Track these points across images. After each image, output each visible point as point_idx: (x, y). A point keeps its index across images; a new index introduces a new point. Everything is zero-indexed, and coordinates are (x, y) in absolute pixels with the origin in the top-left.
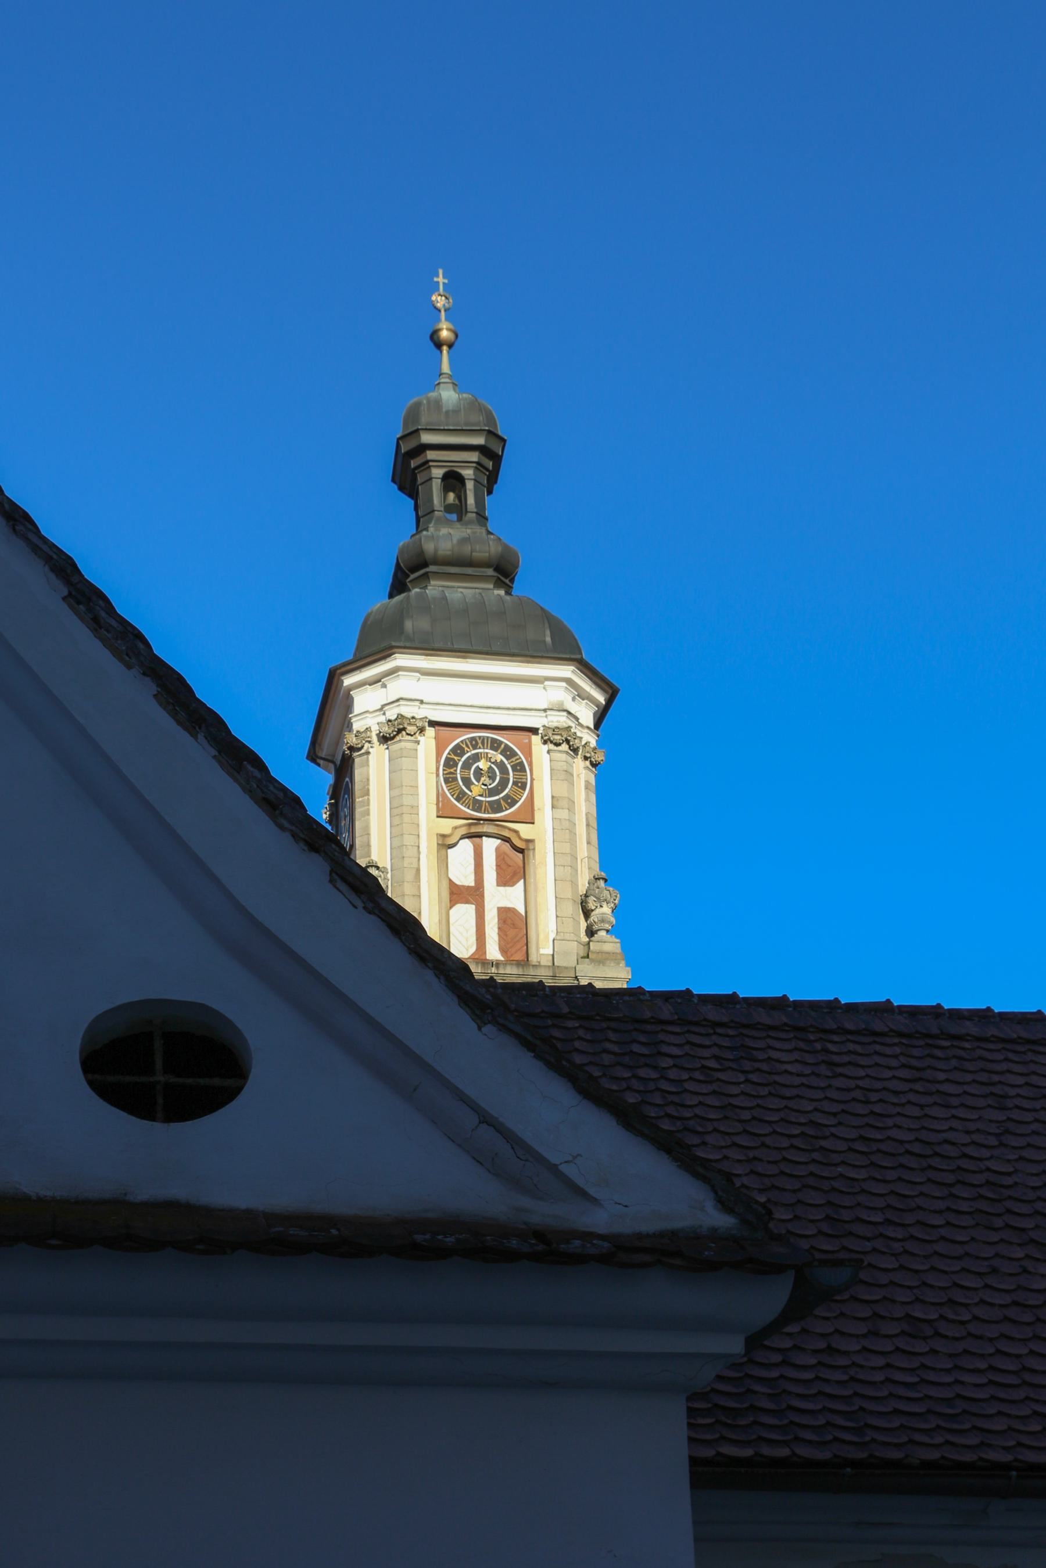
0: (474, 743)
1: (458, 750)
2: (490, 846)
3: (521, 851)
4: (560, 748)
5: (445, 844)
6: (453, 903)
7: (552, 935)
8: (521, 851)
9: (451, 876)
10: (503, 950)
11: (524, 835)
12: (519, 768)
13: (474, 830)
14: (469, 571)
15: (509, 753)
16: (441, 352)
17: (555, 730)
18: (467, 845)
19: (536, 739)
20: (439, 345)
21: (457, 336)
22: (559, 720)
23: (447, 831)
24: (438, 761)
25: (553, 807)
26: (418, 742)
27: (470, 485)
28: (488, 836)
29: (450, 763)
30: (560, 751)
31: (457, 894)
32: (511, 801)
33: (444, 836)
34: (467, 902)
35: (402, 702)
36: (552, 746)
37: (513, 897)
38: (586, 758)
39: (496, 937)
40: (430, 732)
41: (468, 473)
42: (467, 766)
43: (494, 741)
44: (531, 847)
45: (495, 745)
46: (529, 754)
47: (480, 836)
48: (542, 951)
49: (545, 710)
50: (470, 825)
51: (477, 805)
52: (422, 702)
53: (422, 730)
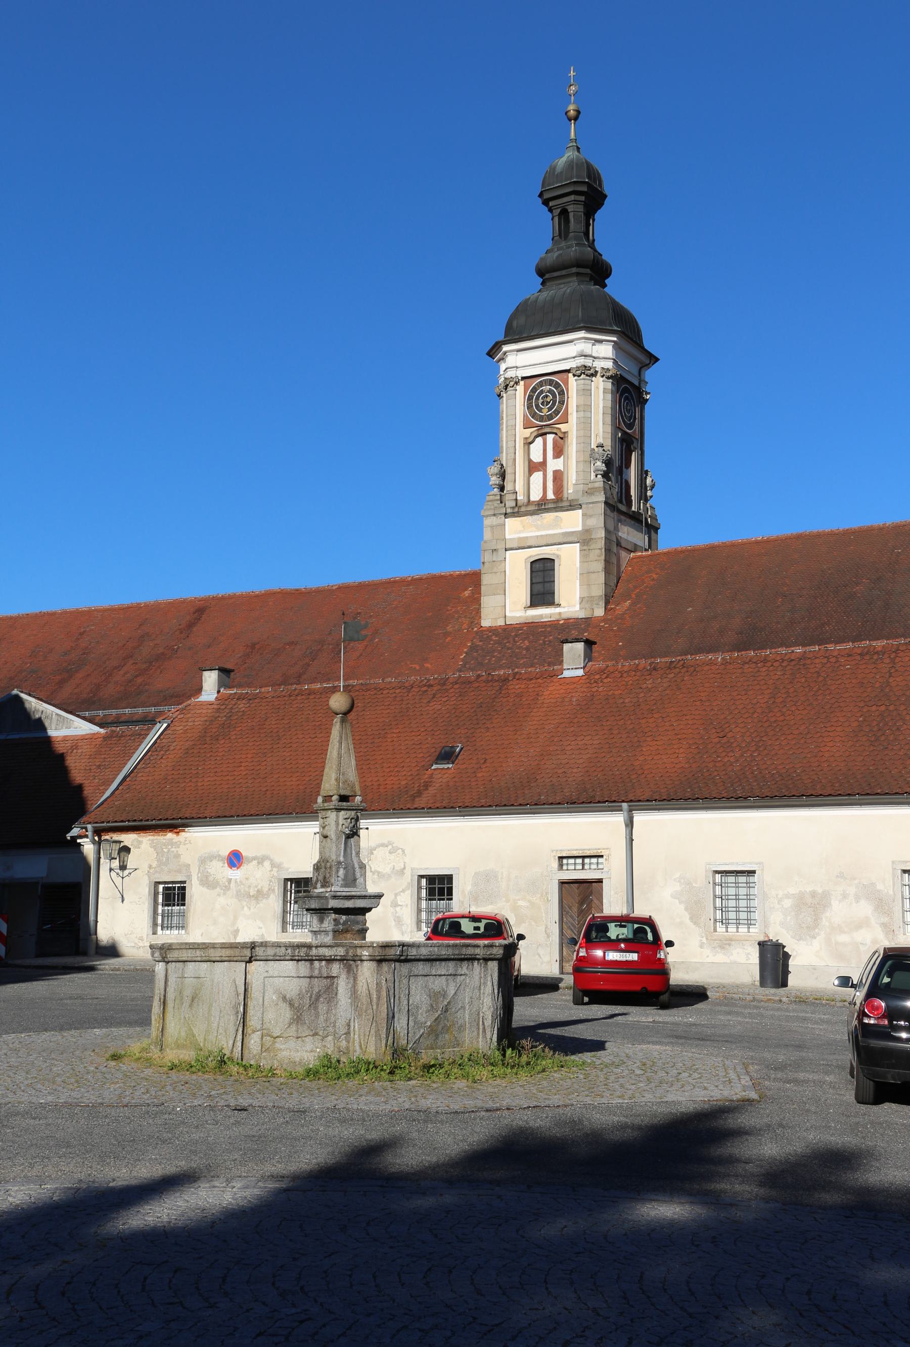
0: (541, 384)
1: (534, 390)
2: (550, 438)
3: (562, 438)
4: (581, 377)
5: (528, 443)
6: (530, 474)
7: (574, 482)
8: (562, 438)
9: (532, 457)
10: (554, 494)
11: (563, 430)
12: (562, 393)
13: (540, 432)
14: (564, 272)
15: (557, 386)
16: (571, 124)
17: (578, 368)
18: (539, 440)
19: (570, 375)
20: (570, 120)
21: (578, 112)
22: (581, 361)
23: (528, 435)
24: (525, 398)
25: (577, 412)
26: (516, 390)
27: (571, 215)
28: (550, 433)
29: (530, 398)
30: (581, 379)
31: (533, 467)
32: (557, 412)
33: (526, 438)
34: (539, 470)
35: (508, 370)
36: (576, 378)
37: (554, 464)
38: (602, 376)
39: (552, 487)
40: (522, 383)
41: (570, 208)
42: (537, 398)
43: (551, 380)
44: (566, 436)
45: (551, 382)
46: (566, 384)
47: (545, 434)
48: (569, 492)
49: (574, 358)
50: (538, 430)
51: (541, 419)
52: (517, 367)
53: (517, 383)
